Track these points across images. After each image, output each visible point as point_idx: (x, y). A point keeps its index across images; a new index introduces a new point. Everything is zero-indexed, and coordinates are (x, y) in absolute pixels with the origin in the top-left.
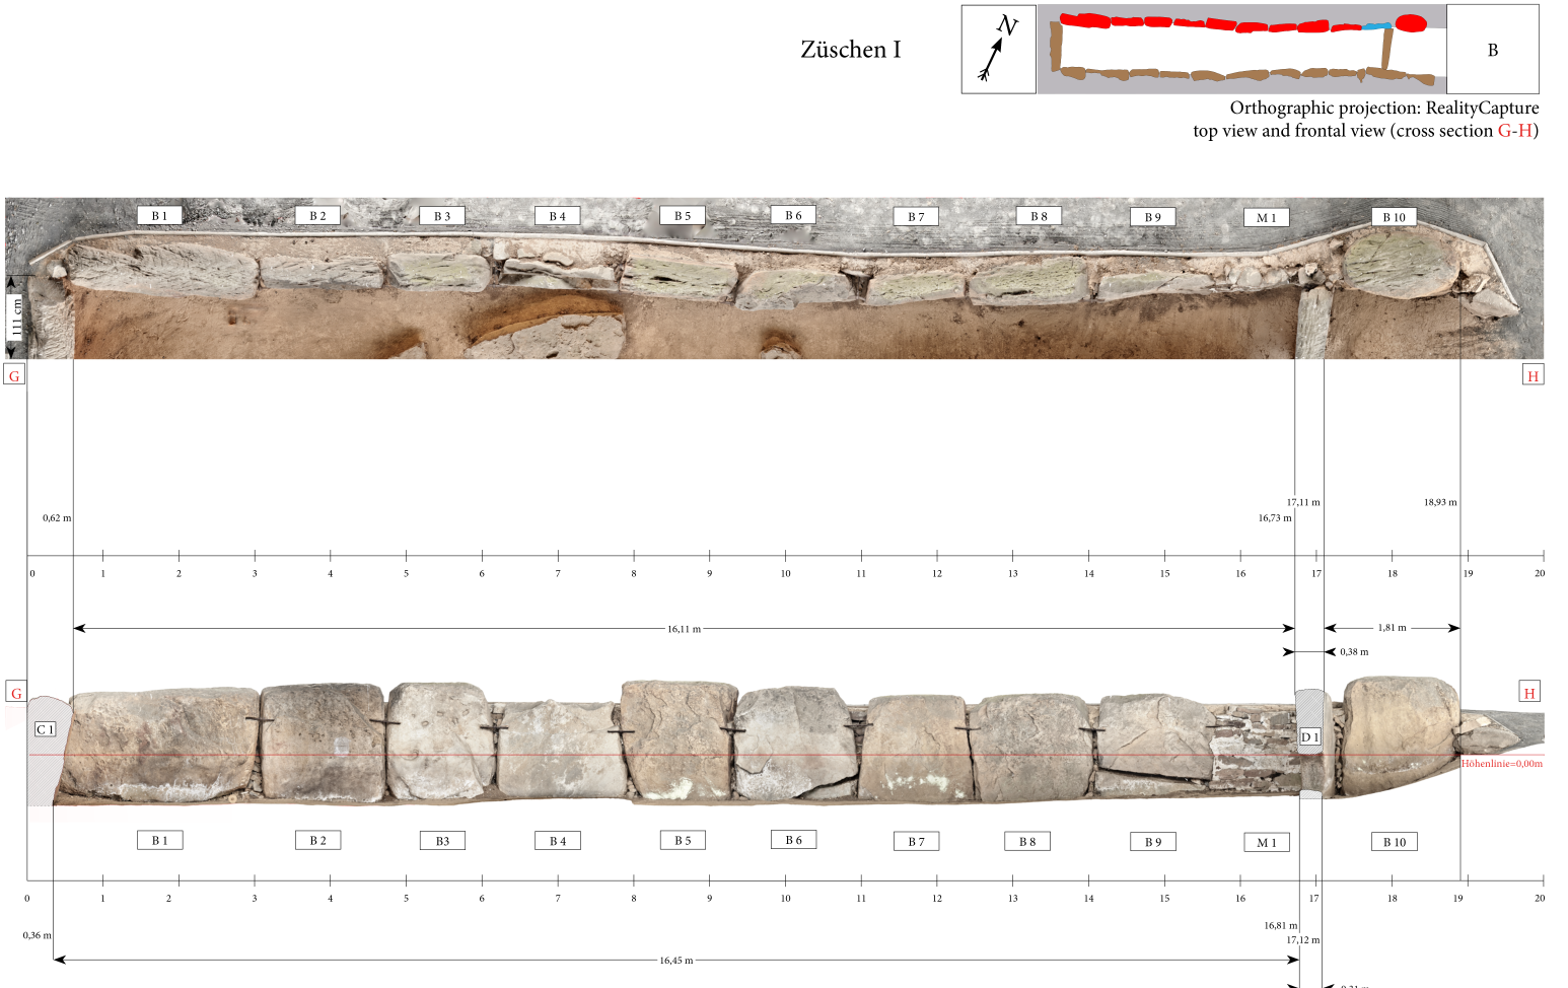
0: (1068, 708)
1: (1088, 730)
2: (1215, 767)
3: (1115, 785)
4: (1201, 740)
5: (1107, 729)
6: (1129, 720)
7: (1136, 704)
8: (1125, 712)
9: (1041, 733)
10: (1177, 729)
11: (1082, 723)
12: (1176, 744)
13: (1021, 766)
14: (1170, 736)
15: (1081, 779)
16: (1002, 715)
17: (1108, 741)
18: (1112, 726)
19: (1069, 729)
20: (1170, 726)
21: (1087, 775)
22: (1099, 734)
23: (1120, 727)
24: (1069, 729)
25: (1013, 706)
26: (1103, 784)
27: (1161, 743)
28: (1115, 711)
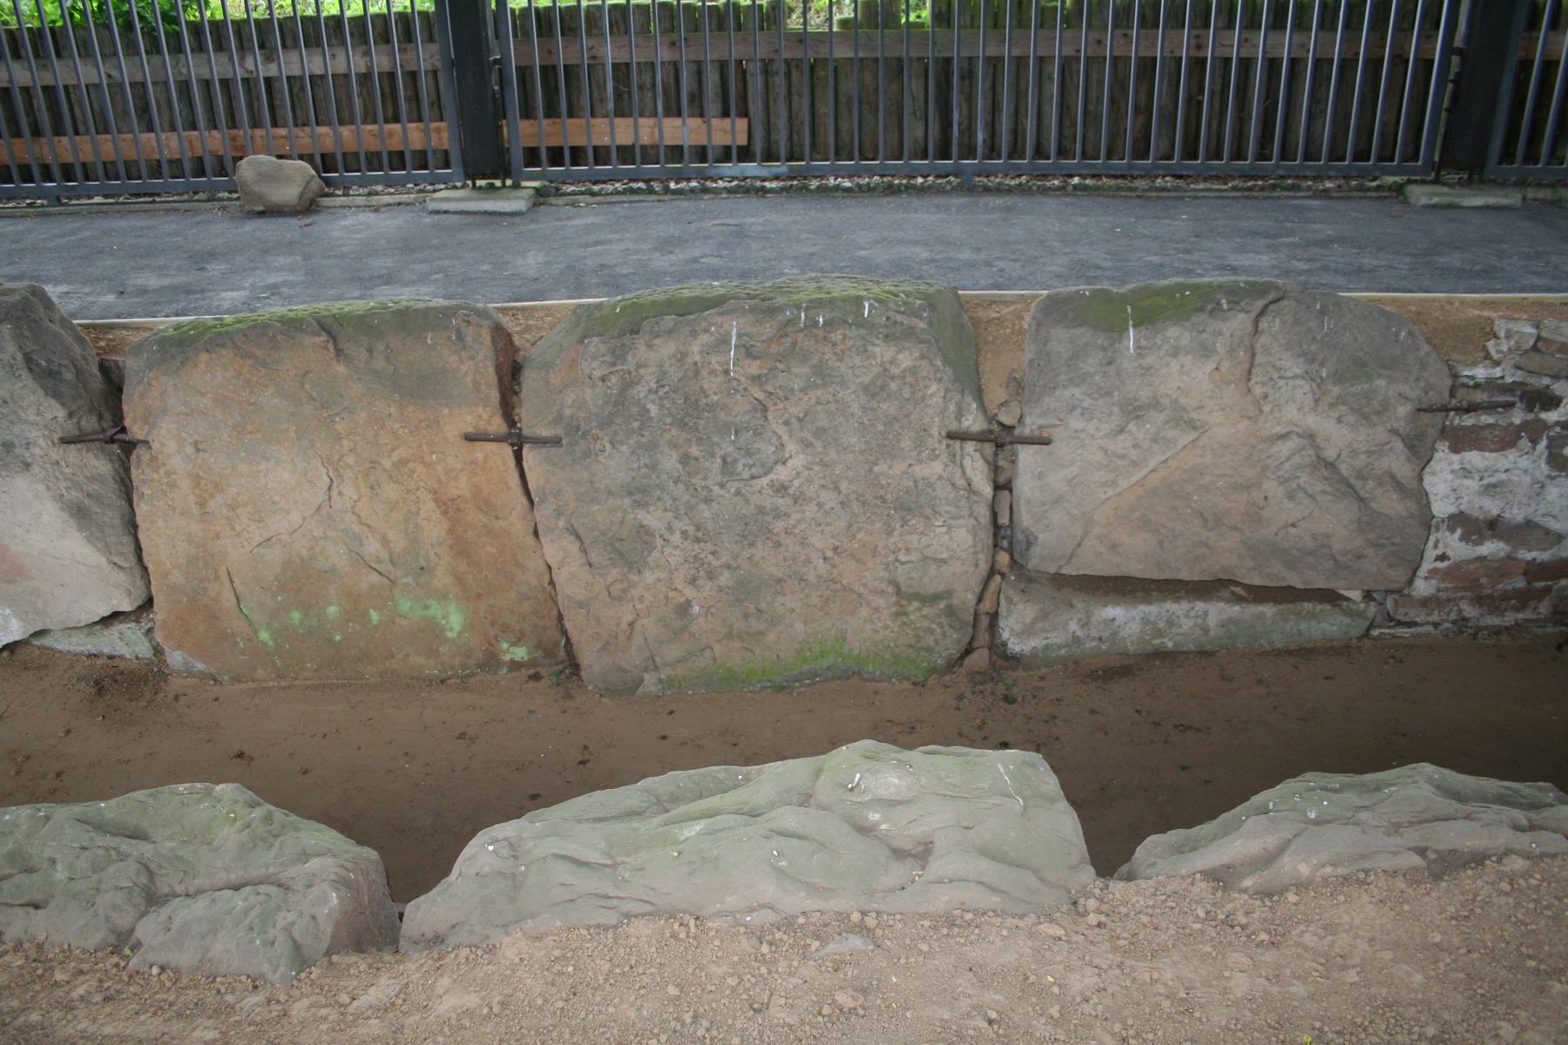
0: (906, 359)
1: (980, 438)
2: (1431, 553)
3: (1074, 626)
4: (1398, 462)
5: (1058, 434)
6: (1144, 394)
7: (1173, 332)
8: (1128, 366)
9: (798, 462)
10: (1311, 421)
11: (959, 414)
12: (1304, 479)
13: (725, 578)
14: (1285, 448)
15: (951, 612)
16: (641, 391)
17: (1056, 479)
18: (1076, 423)
19: (906, 443)
20: (1291, 413)
21: (971, 598)
22: (1026, 455)
23: (1107, 427)
24: (906, 443)
25: (681, 357)
26: (1028, 631)
27: (1250, 473)
28: (1091, 364)
